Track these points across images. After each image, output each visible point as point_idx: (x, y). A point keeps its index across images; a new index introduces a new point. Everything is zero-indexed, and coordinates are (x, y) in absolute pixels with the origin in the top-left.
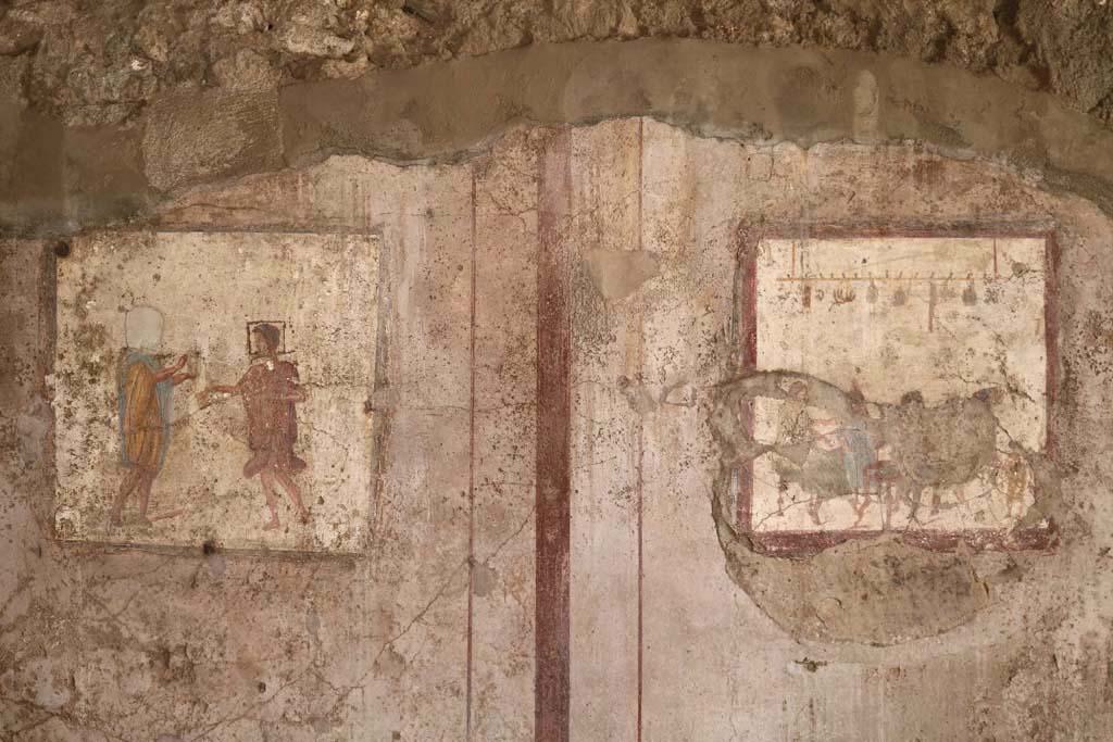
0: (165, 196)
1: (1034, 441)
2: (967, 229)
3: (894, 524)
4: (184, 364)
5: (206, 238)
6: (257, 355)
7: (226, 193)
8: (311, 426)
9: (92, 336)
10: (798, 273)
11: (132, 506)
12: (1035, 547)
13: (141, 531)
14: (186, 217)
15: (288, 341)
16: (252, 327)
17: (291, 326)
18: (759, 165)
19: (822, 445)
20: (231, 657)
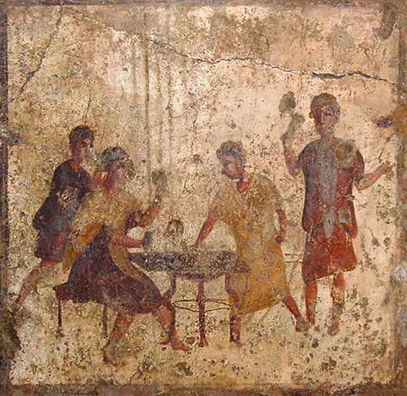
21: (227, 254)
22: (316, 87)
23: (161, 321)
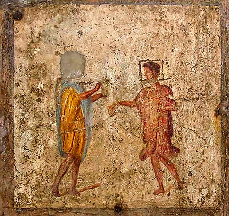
4: (99, 89)
5: (111, 8)
13: (73, 199)
15: (165, 72)
16: (142, 64)
17: (167, 63)
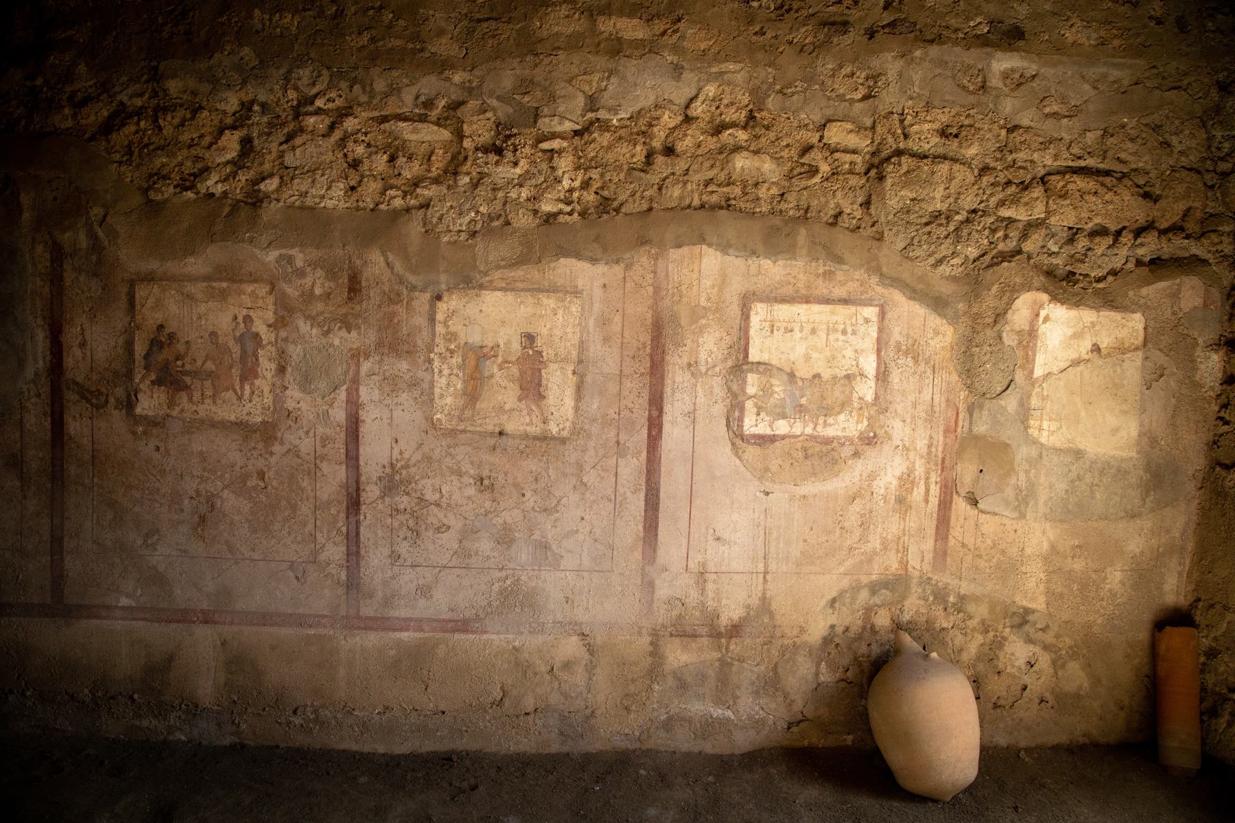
0: (486, 274)
1: (869, 398)
2: (845, 301)
3: (806, 432)
6: (525, 348)
7: (512, 274)
8: (548, 380)
9: (451, 337)
10: (769, 318)
11: (468, 413)
12: (867, 444)
14: (495, 284)
15: (539, 342)
18: (753, 269)
19: (776, 396)
20: (510, 482)
21: (213, 372)
22: (245, 312)
23: (188, 394)
